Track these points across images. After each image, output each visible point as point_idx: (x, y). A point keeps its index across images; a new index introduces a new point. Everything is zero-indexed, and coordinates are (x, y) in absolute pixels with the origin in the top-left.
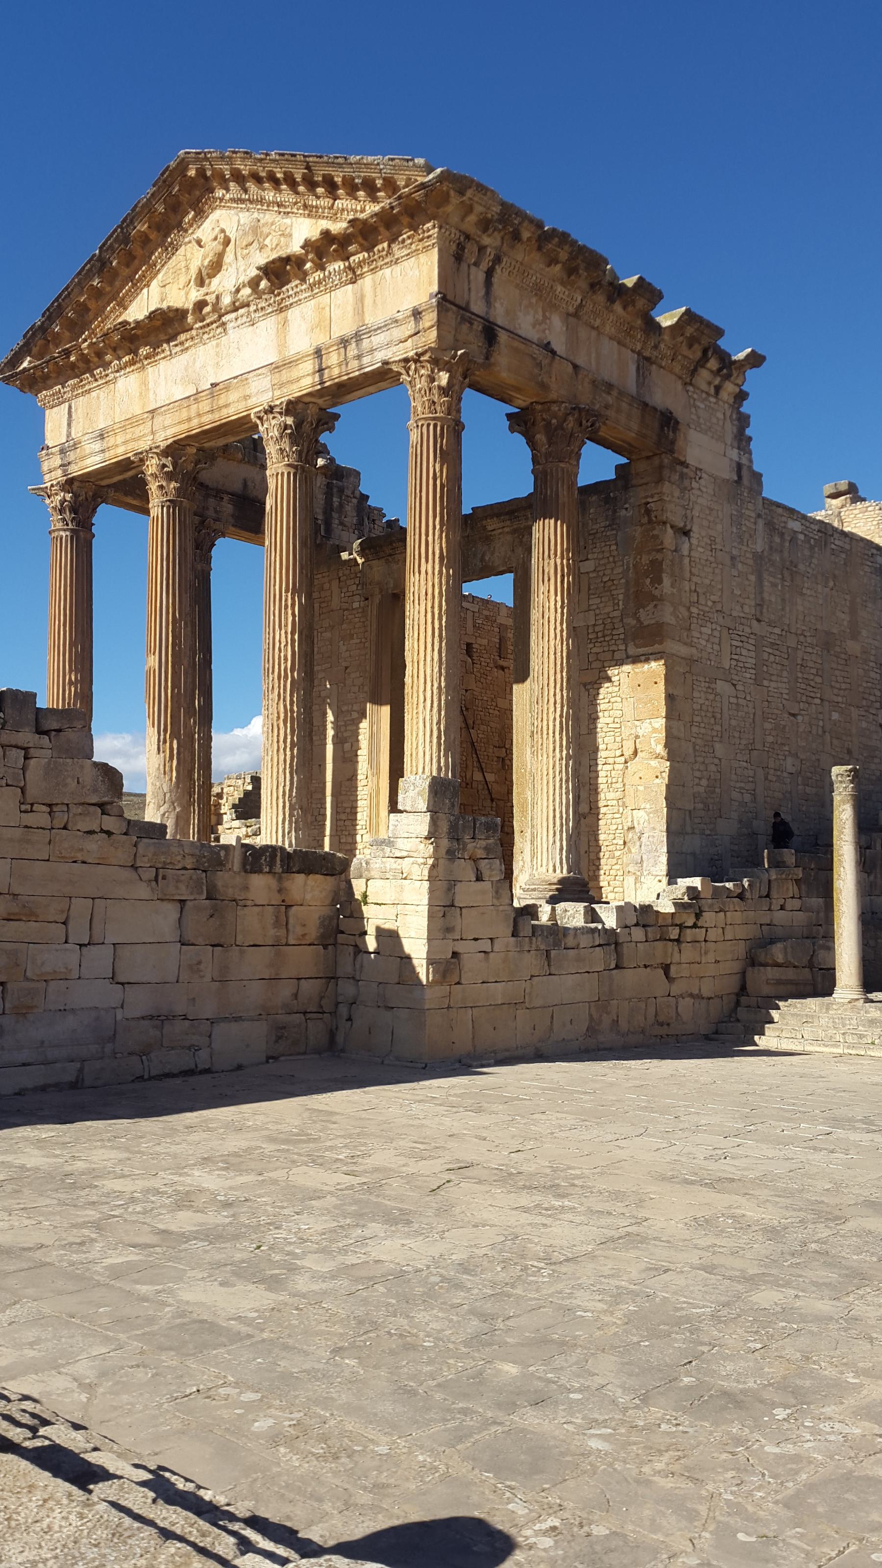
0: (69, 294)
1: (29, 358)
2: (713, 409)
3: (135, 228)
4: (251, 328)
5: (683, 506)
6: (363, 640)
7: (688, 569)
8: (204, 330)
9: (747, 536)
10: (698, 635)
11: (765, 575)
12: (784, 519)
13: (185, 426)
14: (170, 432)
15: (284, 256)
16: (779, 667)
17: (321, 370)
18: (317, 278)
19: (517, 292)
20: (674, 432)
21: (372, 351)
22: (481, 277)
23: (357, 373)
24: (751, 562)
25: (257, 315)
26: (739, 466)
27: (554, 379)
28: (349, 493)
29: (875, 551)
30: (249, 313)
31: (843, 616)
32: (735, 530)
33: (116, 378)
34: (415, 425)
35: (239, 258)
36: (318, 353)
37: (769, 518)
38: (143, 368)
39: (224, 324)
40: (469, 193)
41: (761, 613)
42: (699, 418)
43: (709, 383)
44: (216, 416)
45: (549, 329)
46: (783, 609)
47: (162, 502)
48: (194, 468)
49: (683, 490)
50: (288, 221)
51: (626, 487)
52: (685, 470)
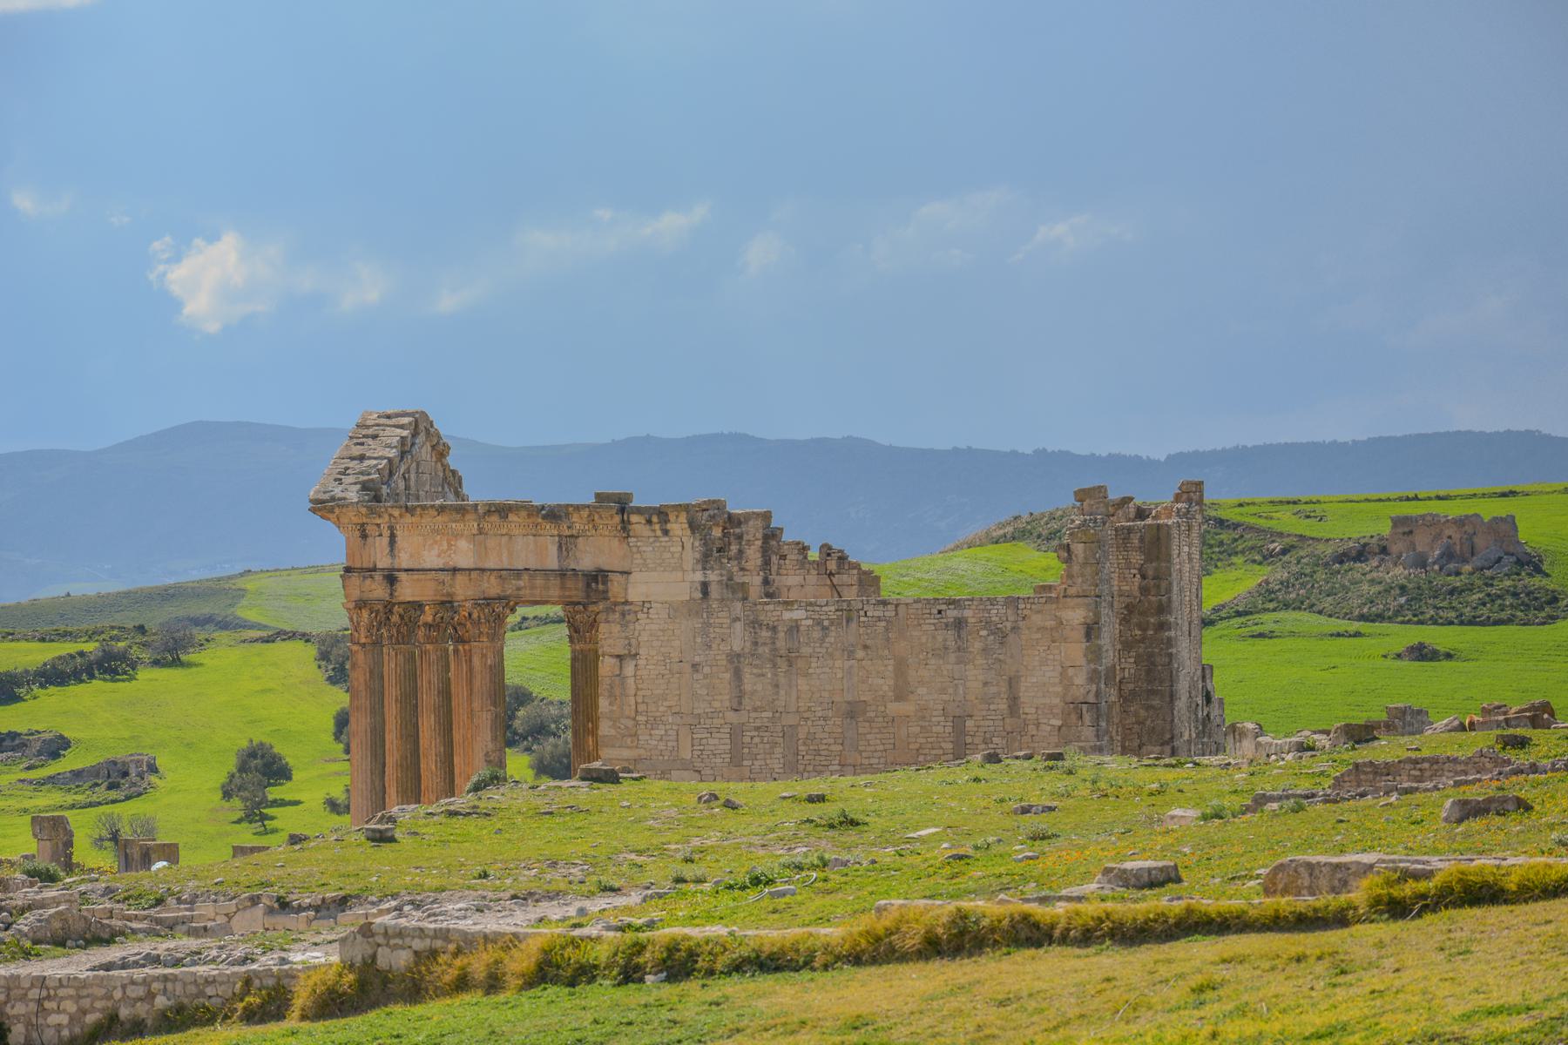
2: (665, 547)
5: (627, 638)
7: (634, 687)
9: (718, 641)
10: (648, 737)
11: (747, 670)
12: (779, 613)
16: (767, 746)
19: (420, 538)
20: (605, 583)
22: (385, 540)
24: (725, 663)
26: (705, 587)
27: (458, 587)
28: (750, 537)
29: (943, 607)
31: (881, 681)
32: (699, 640)
37: (751, 618)
40: (337, 511)
41: (740, 703)
42: (645, 560)
43: (654, 531)
45: (455, 553)
46: (777, 693)
48: (434, 620)
49: (625, 626)
52: (627, 608)
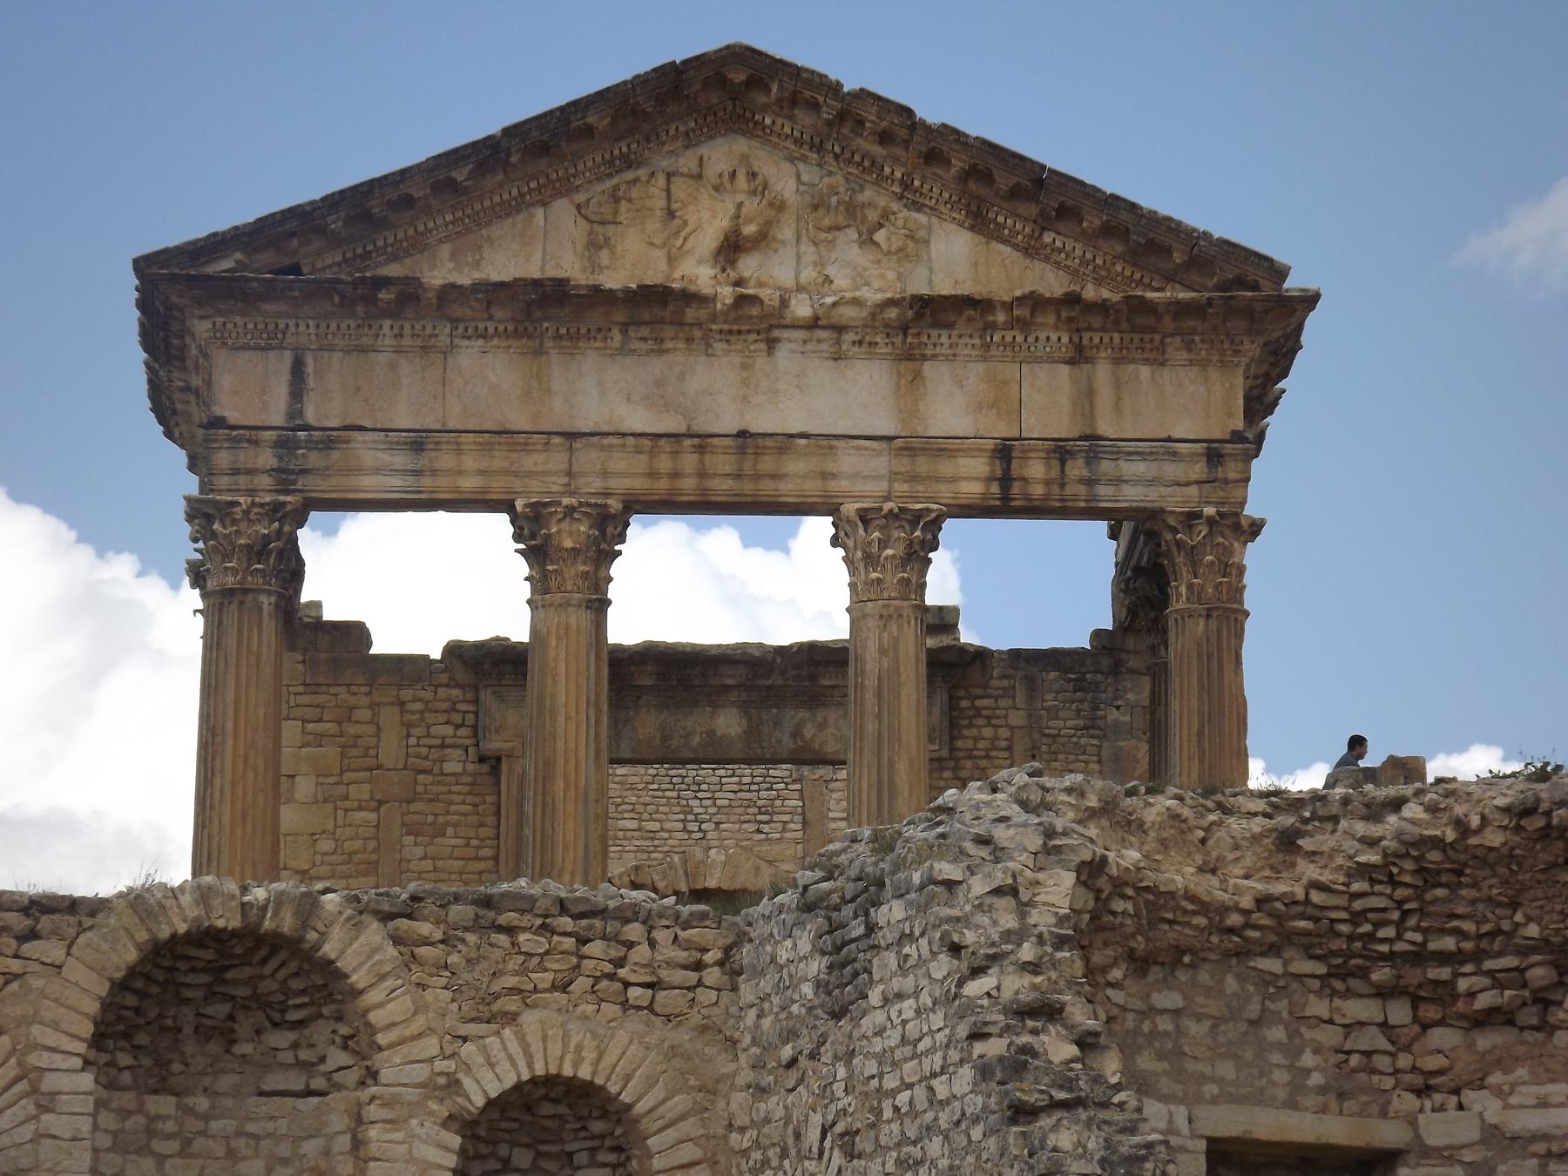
0: (402, 181)
1: (238, 256)
3: (584, 117)
4: (831, 363)
6: (474, 842)
8: (722, 337)
13: (663, 484)
14: (614, 483)
15: (977, 297)
17: (1006, 480)
18: (1009, 339)
21: (1118, 481)
23: (1083, 504)
25: (856, 349)
30: (838, 342)
33: (453, 346)
35: (804, 239)
36: (1004, 452)
38: (539, 352)
39: (776, 340)
44: (748, 487)
47: (589, 601)
50: (922, 218)
51: (1116, 670)
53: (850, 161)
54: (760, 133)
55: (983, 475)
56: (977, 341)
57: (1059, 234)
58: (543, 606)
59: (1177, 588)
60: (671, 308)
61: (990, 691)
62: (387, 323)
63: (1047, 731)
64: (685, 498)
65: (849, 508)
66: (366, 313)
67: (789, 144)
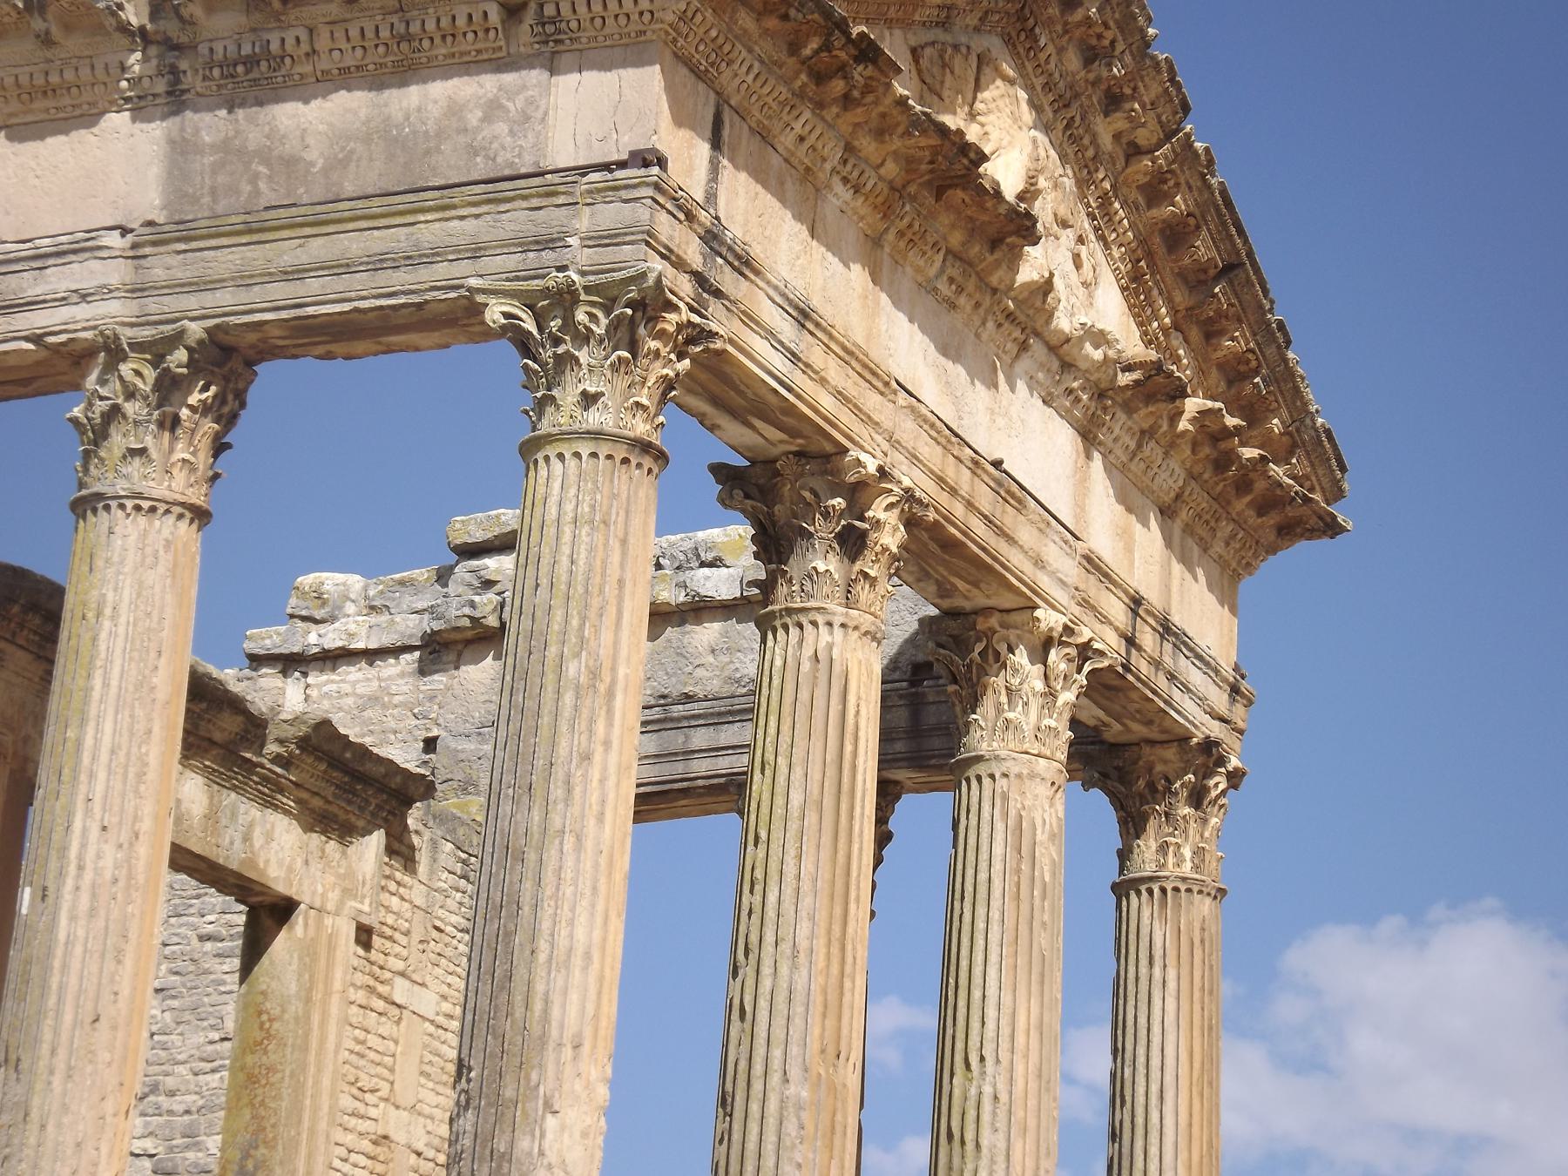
17: (1131, 641)
21: (1186, 689)
34: (1213, 893)
53: (1073, 139)
54: (1022, 51)
55: (1122, 627)
56: (1133, 445)
57: (1186, 340)
58: (843, 625)
59: (1178, 846)
60: (997, 255)
61: (403, 849)
62: (807, 115)
63: (438, 923)
64: (953, 530)
65: (1049, 619)
66: (804, 85)
67: (1039, 82)
